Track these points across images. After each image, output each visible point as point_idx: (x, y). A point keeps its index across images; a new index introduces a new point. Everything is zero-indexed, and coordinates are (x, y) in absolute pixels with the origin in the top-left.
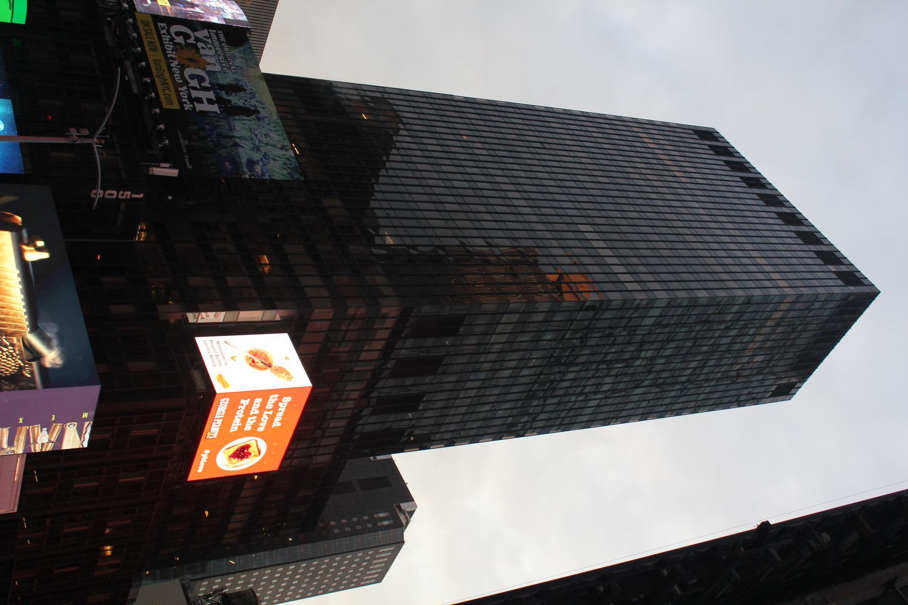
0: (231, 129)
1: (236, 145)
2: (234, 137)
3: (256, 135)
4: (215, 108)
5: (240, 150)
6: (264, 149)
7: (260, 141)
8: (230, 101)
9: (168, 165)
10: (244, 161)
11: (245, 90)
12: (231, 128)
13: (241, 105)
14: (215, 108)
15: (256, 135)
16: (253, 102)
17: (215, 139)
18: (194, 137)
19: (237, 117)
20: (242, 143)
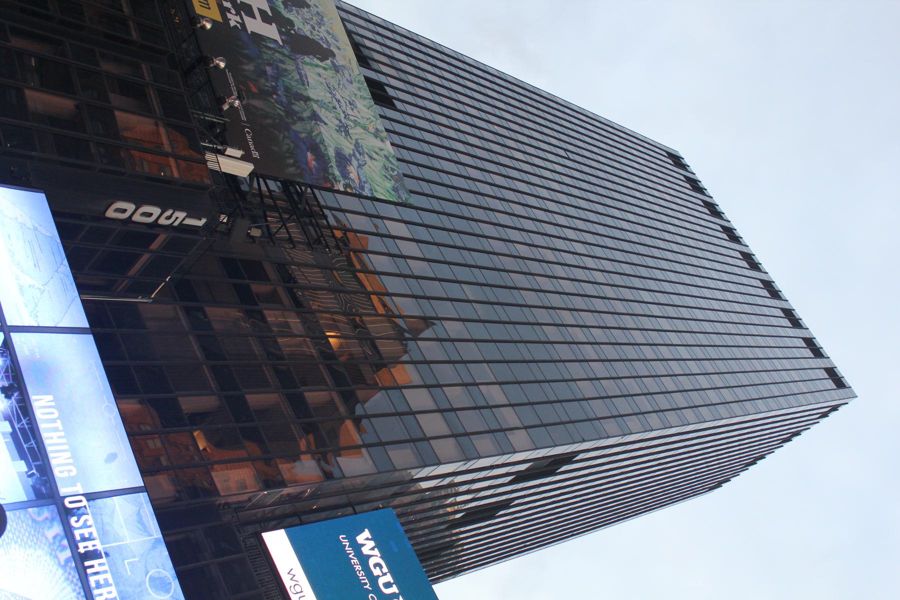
0: (304, 84)
1: (315, 117)
2: (307, 99)
3: (338, 101)
4: (271, 31)
5: (323, 128)
6: (356, 132)
7: (346, 116)
8: (291, 23)
9: (239, 153)
10: (331, 153)
11: (308, 6)
12: (303, 81)
13: (308, 34)
14: (271, 31)
15: (338, 101)
16: (323, 34)
17: (284, 99)
18: (255, 90)
19: (307, 59)
20: (323, 113)
